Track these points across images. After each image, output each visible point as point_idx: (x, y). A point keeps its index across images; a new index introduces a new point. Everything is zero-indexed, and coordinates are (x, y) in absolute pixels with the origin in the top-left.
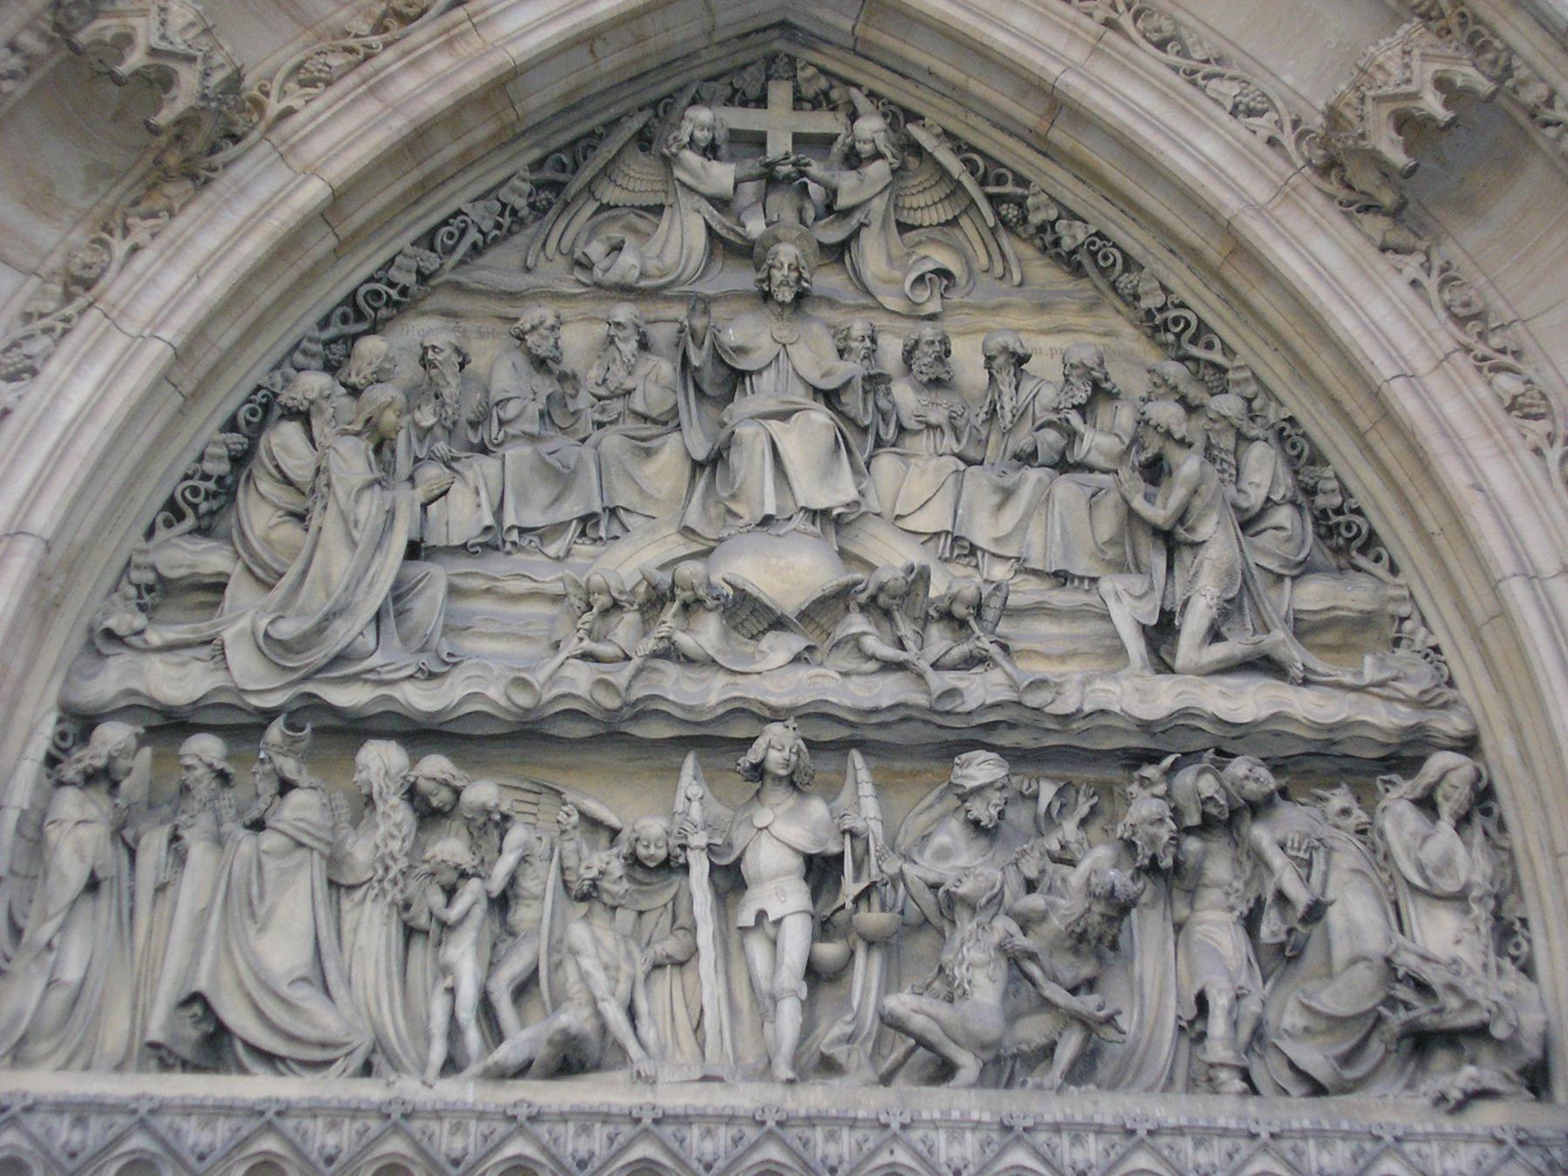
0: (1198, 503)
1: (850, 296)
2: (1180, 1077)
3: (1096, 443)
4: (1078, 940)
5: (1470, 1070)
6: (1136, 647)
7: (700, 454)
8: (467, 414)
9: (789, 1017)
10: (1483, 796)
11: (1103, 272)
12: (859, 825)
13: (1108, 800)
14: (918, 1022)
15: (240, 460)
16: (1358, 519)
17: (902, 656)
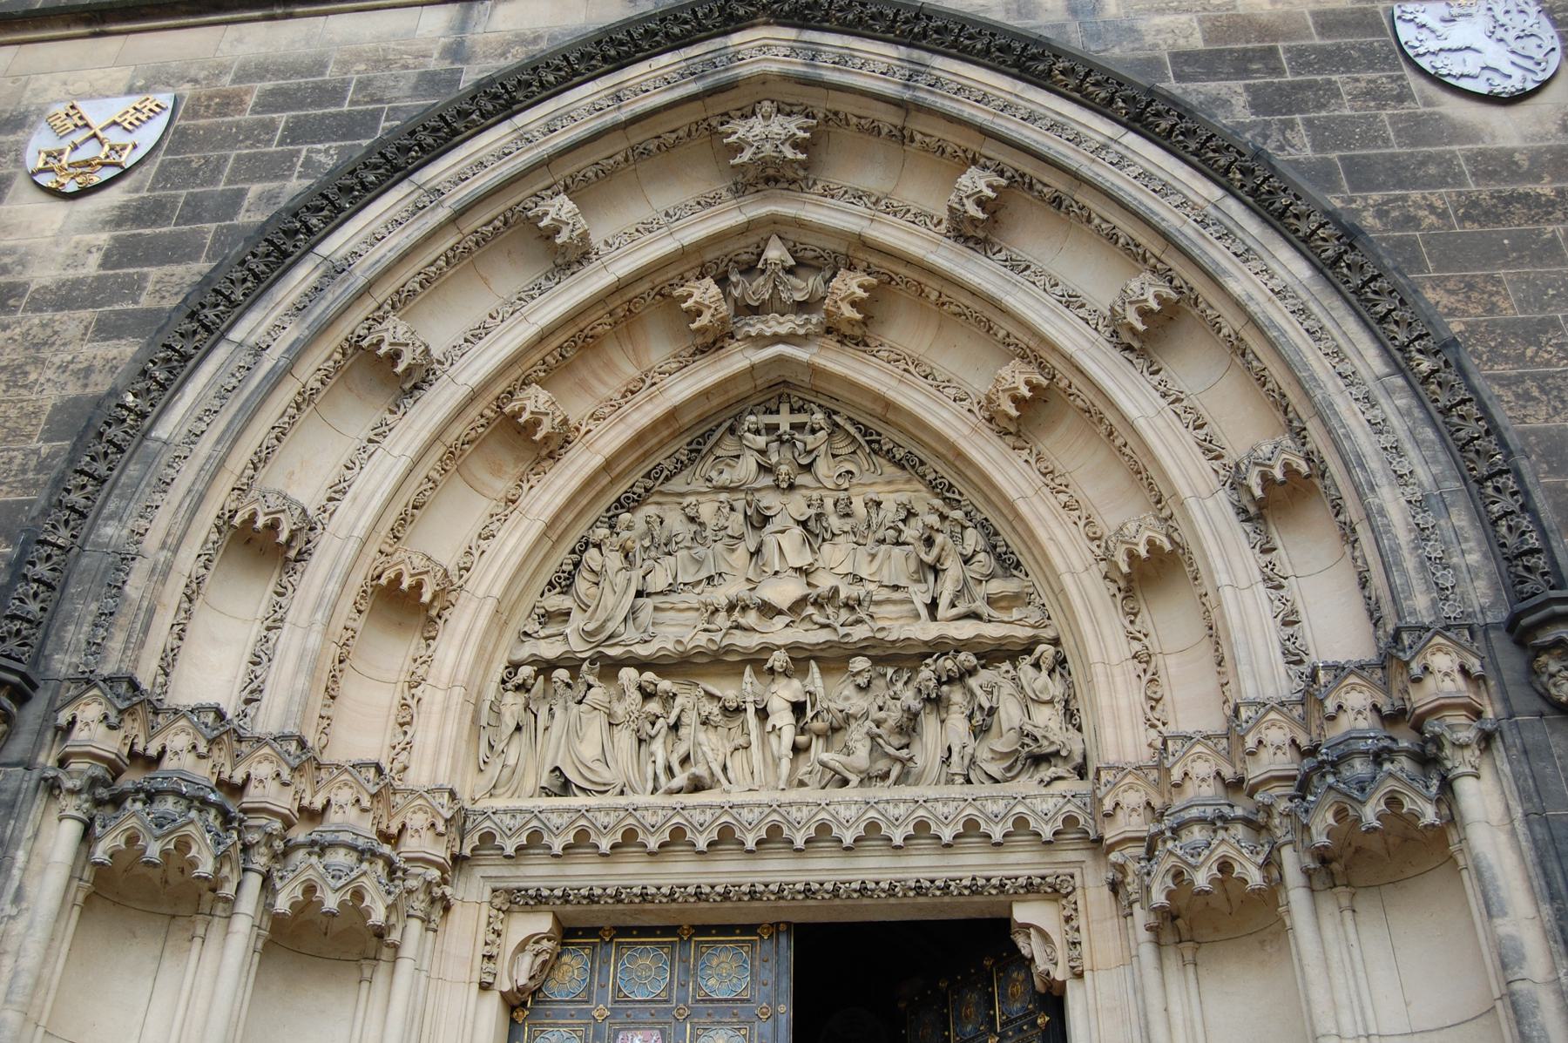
0: (944, 553)
1: (814, 484)
2: (943, 779)
3: (911, 532)
4: (901, 730)
5: (1053, 769)
6: (924, 612)
7: (752, 550)
8: (663, 541)
9: (785, 765)
10: (1061, 662)
11: (913, 467)
12: (812, 689)
13: (915, 671)
14: (832, 764)
15: (576, 565)
17: (828, 622)
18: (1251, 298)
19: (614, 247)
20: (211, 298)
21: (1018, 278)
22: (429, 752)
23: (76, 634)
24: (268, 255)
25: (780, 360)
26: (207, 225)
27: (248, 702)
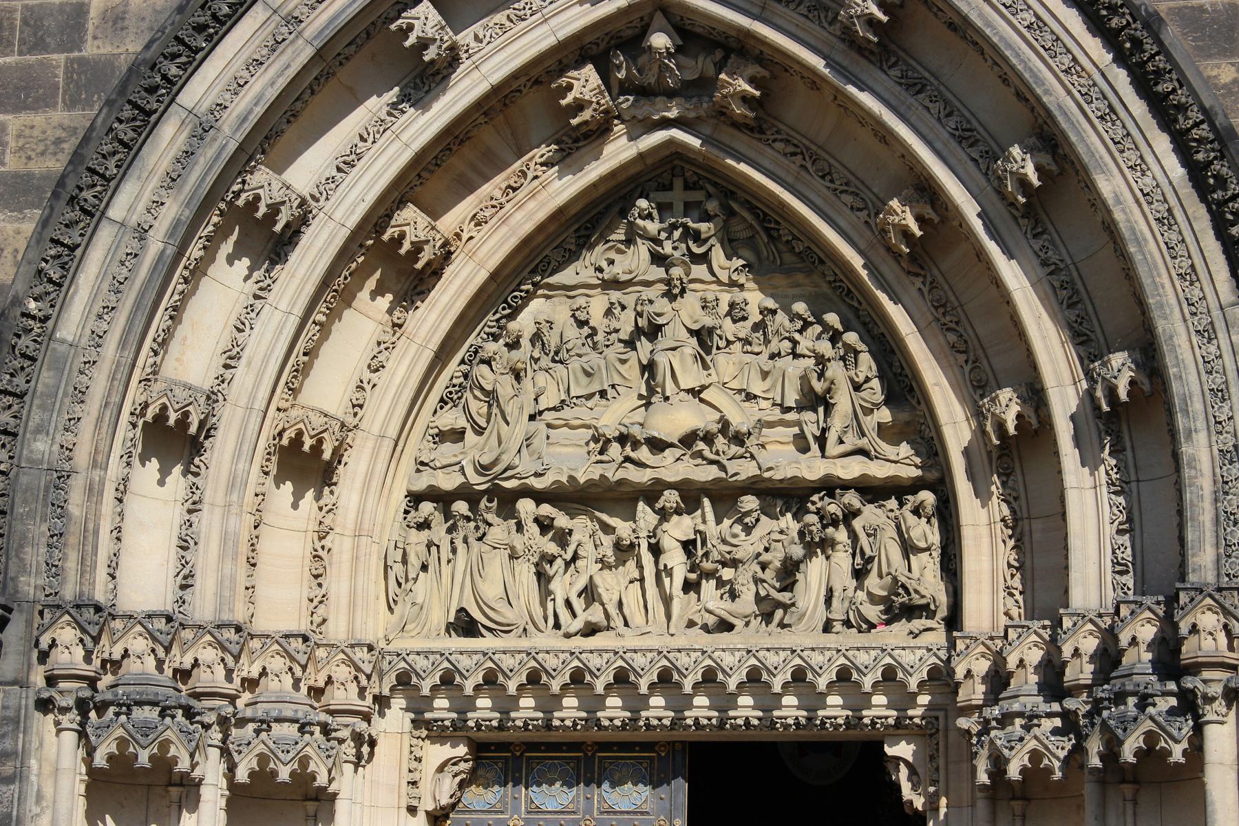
12: (701, 527)
16: (906, 380)
17: (717, 458)
18: (1118, 201)
19: (485, 42)
20: (87, 179)
21: (912, 100)
22: (344, 601)
23: (35, 555)
24: (134, 119)
25: (671, 142)
26: (55, 56)
27: (183, 587)
